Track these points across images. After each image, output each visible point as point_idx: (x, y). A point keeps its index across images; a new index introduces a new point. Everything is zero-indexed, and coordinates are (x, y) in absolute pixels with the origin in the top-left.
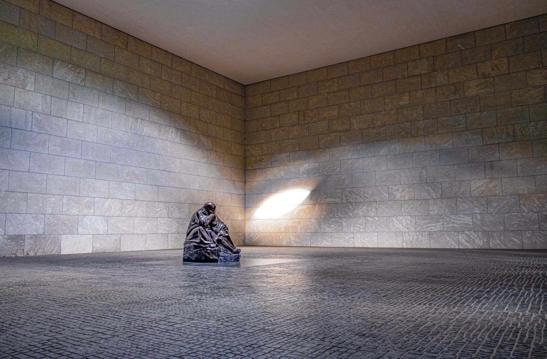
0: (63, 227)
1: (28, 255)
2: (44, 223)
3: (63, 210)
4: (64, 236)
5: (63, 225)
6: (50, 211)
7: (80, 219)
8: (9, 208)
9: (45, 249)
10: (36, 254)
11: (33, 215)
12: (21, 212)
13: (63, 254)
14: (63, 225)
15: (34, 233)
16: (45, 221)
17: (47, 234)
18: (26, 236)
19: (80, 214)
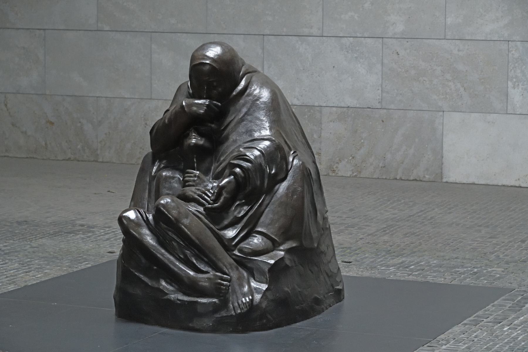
0: (450, 84)
1: (334, 171)
2: (379, 66)
3: (449, 21)
4: (457, 116)
5: (448, 76)
6: (400, 28)
7: (516, 55)
8: (270, 19)
9: (389, 156)
10: (360, 172)
11: (344, 40)
12: (306, 31)
13: (451, 180)
14: (448, 76)
15: (350, 101)
16: (385, 61)
17: (392, 106)
18: (325, 110)
19: (514, 38)
